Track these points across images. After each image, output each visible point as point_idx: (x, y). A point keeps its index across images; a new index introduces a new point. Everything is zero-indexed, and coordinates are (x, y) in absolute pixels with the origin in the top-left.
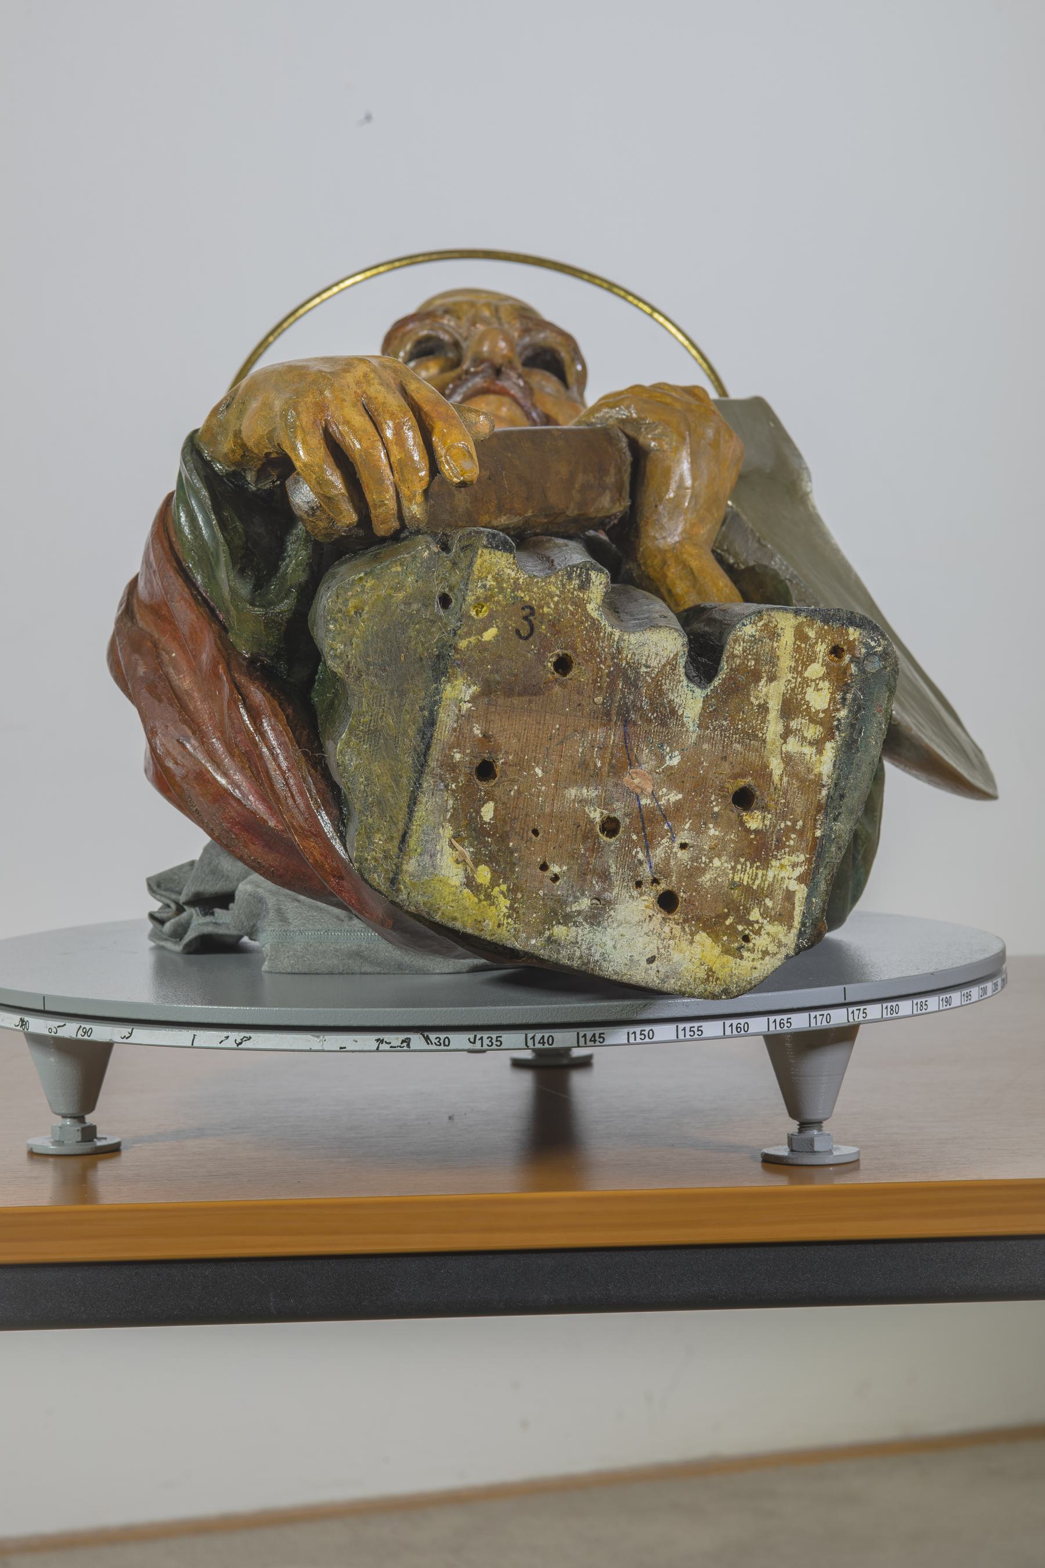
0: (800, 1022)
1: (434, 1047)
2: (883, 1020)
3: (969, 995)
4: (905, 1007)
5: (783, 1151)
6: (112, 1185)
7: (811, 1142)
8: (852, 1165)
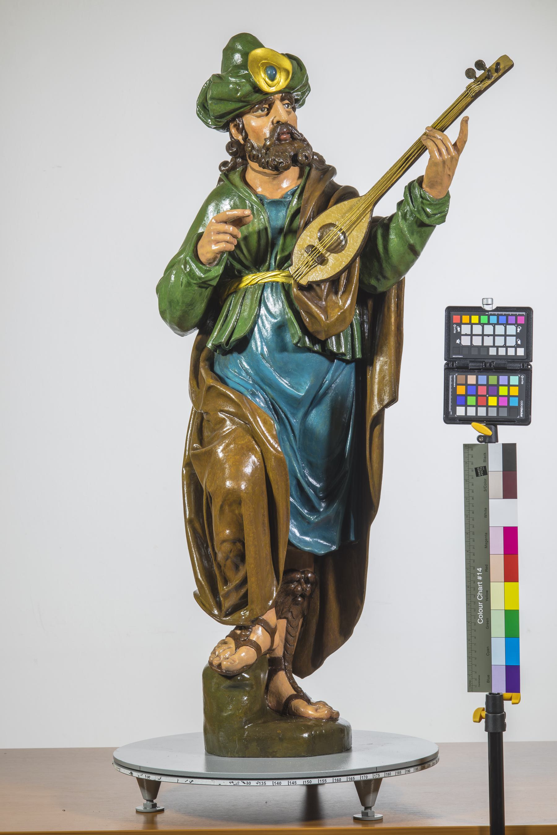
5: (359, 816)
7: (367, 813)
8: (380, 820)
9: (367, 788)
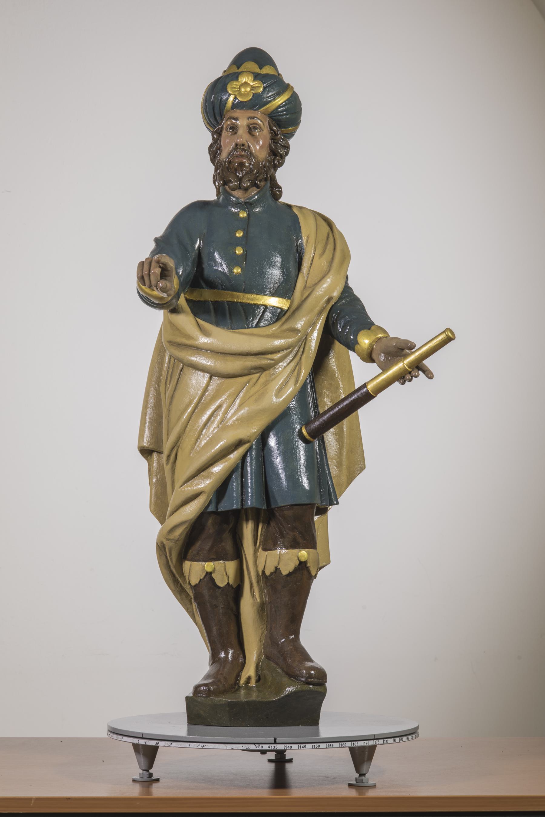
0: (360, 744)
1: (258, 748)
3: (408, 738)
4: (390, 741)
5: (354, 783)
6: (157, 791)
8: (374, 786)
9: (362, 756)
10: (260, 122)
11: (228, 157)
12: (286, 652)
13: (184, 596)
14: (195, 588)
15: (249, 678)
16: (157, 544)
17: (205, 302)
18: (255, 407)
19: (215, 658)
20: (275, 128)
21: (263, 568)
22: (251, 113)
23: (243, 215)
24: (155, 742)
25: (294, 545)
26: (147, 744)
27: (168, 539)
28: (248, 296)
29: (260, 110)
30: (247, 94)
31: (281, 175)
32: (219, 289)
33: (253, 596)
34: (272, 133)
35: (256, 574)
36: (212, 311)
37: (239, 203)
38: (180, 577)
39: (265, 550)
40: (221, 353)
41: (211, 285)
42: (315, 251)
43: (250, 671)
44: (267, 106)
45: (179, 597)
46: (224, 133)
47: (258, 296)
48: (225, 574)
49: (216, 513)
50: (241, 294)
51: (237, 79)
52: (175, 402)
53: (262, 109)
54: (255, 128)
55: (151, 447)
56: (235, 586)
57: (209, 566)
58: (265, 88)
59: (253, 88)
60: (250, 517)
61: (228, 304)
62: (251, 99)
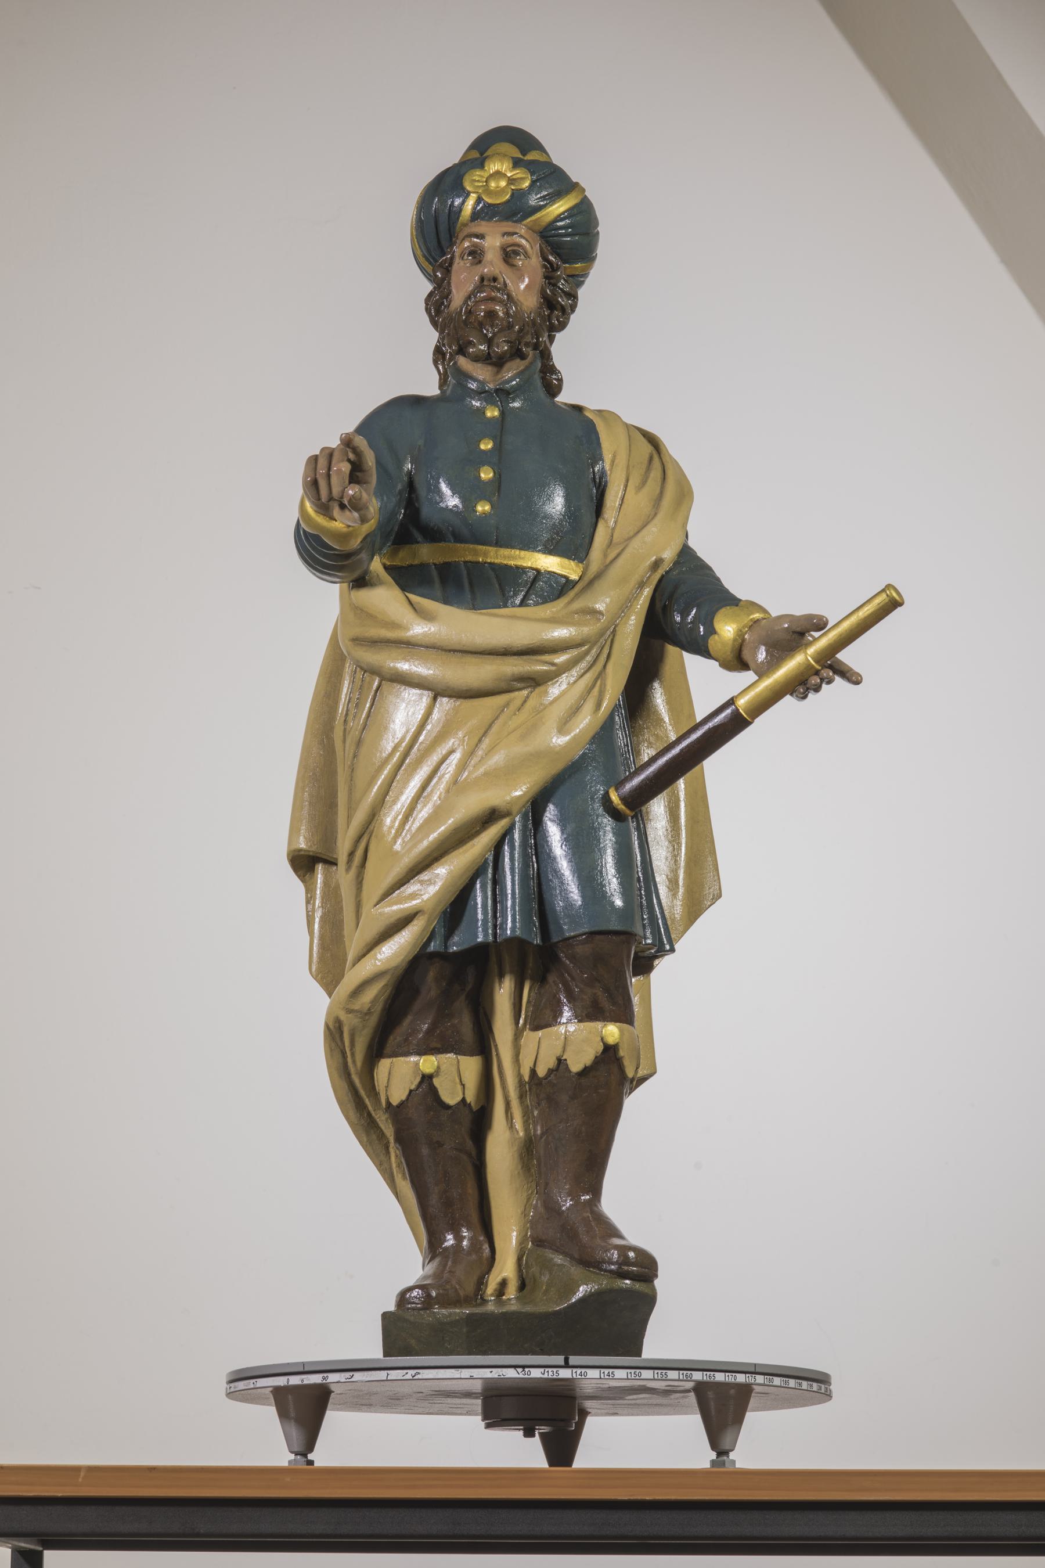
2: (764, 1385)
10: (524, 242)
11: (465, 302)
12: (573, 1231)
13: (374, 1137)
14: (396, 1112)
15: (504, 1283)
16: (327, 1026)
17: (423, 566)
18: (520, 749)
19: (433, 1248)
20: (551, 258)
21: (532, 1065)
22: (508, 226)
23: (492, 413)
24: (321, 1375)
25: (592, 1013)
26: (305, 1382)
27: (349, 1011)
28: (506, 552)
29: (525, 222)
30: (503, 191)
31: (563, 350)
32: (449, 541)
33: (511, 1126)
34: (545, 266)
35: (517, 1080)
36: (437, 580)
37: (486, 392)
38: (368, 1097)
39: (536, 1028)
40: (454, 651)
41: (433, 535)
42: (626, 486)
43: (506, 1268)
44: (538, 215)
45: (365, 1139)
46: (458, 264)
47: (523, 553)
48: (458, 1080)
49: (442, 956)
50: (492, 550)
51: (482, 166)
52: (364, 750)
53: (529, 220)
54: (516, 253)
55: (314, 849)
56: (475, 1107)
57: (428, 1063)
58: (533, 182)
59: (511, 181)
60: (507, 968)
61: (468, 569)
62: (508, 201)
